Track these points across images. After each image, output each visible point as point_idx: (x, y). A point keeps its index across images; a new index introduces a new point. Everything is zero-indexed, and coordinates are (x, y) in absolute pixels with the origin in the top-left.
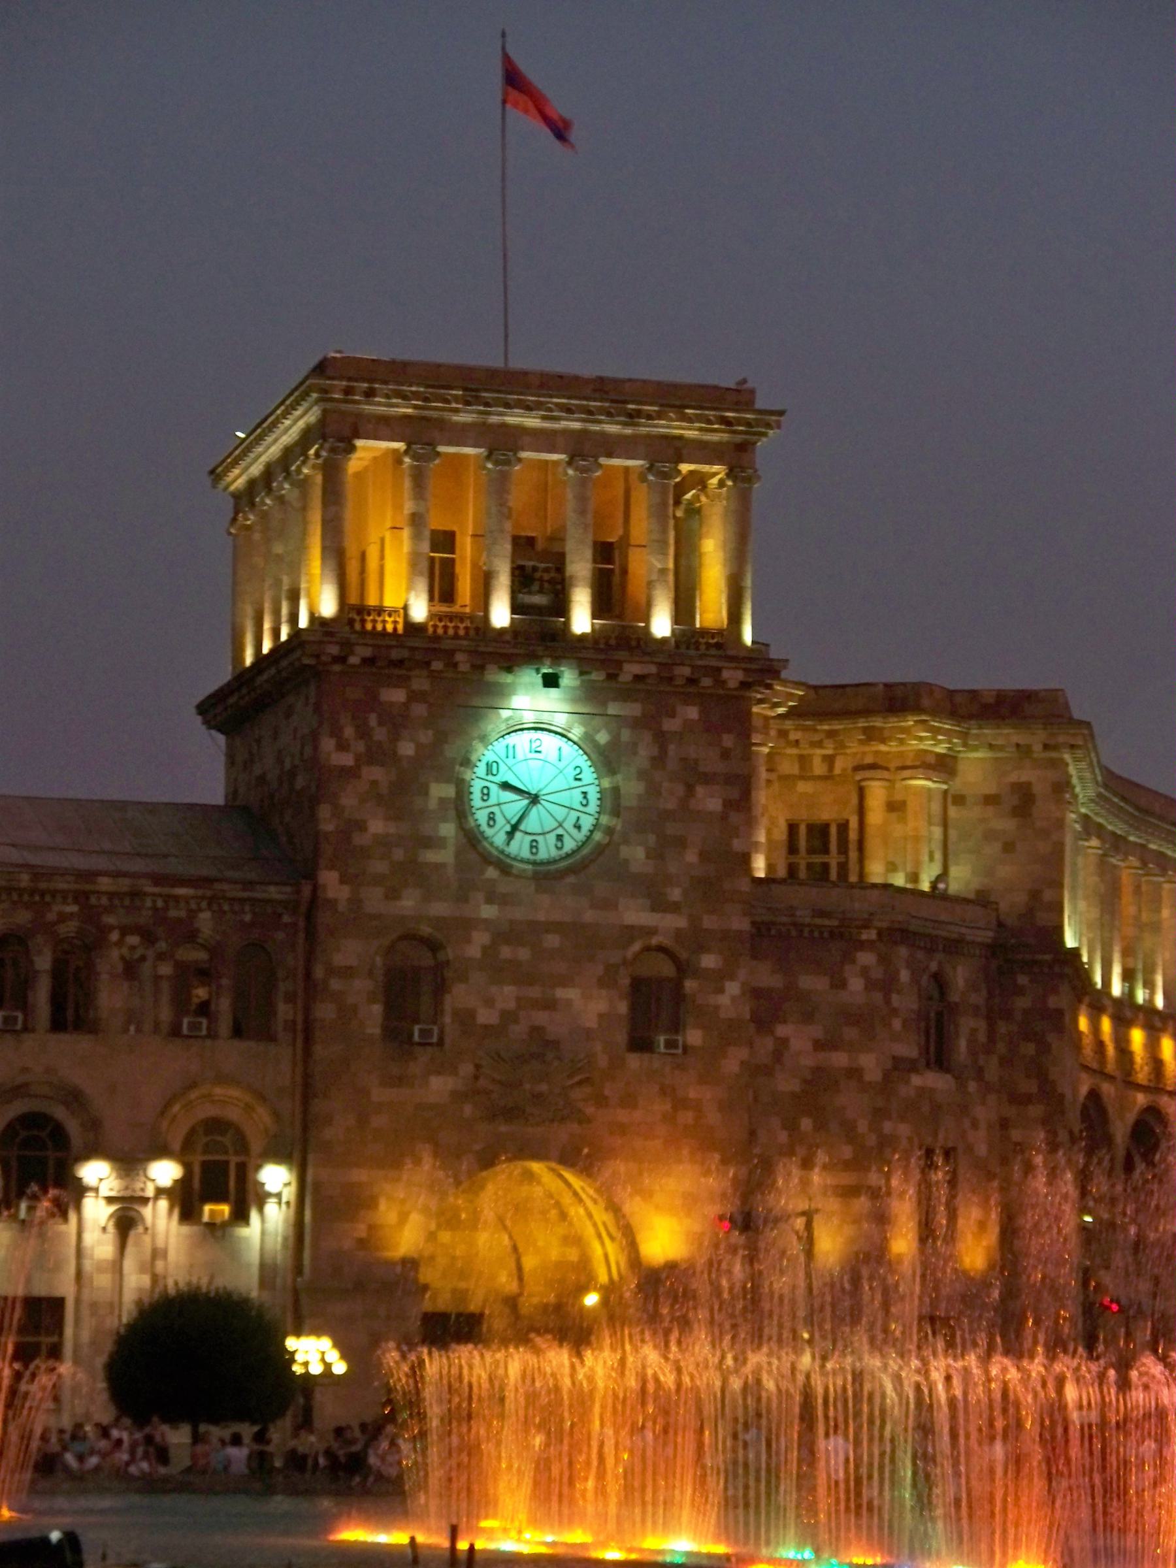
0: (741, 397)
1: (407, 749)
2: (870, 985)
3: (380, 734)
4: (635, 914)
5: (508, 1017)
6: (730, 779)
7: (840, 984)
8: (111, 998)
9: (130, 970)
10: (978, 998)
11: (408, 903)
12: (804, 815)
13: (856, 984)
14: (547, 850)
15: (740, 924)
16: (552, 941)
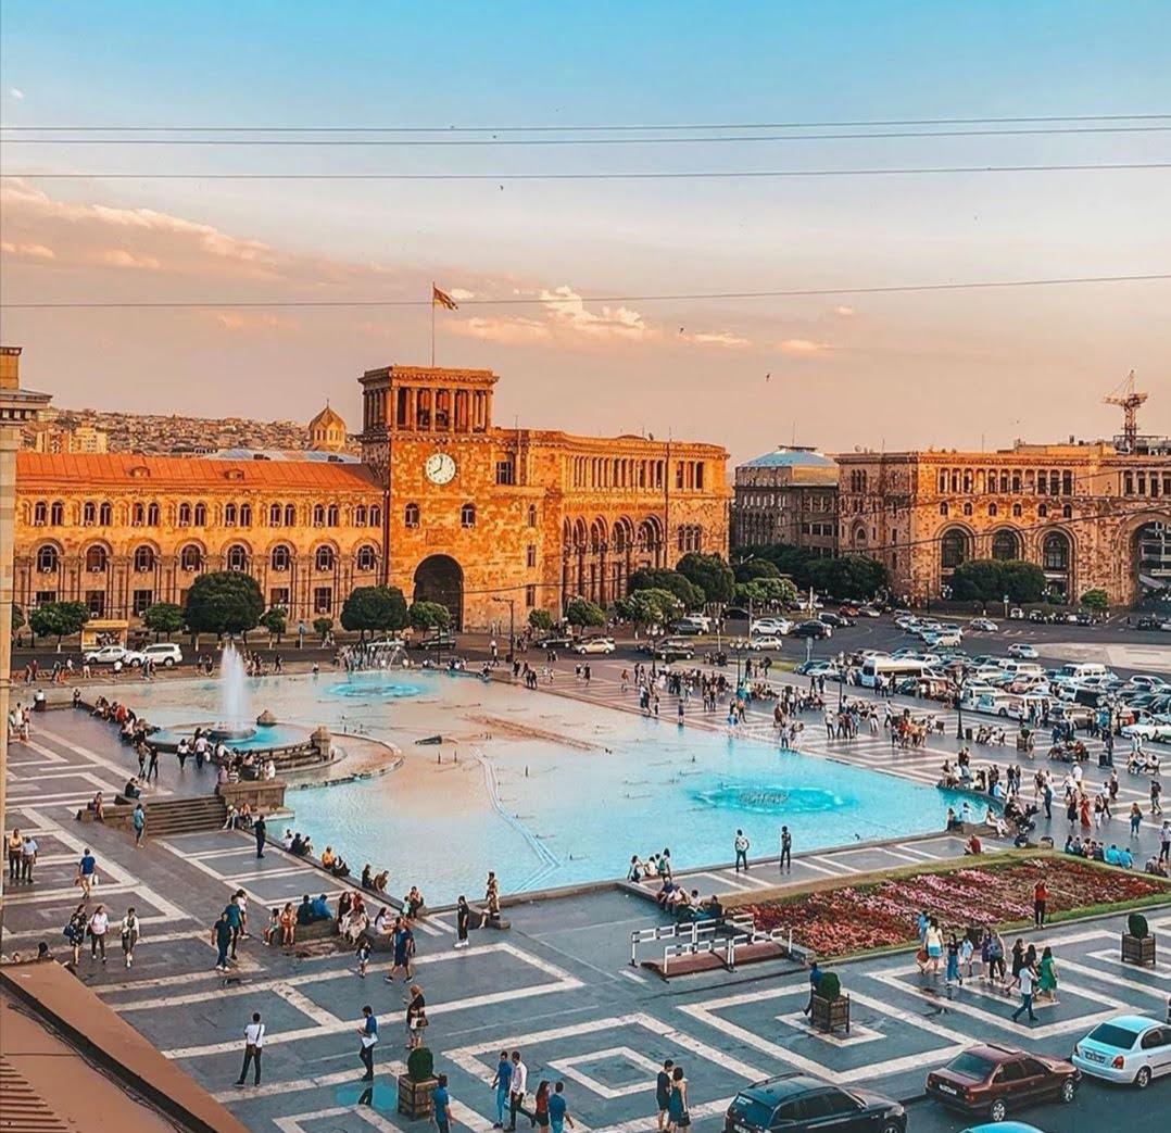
0: (490, 374)
1: (411, 459)
2: (517, 510)
3: (405, 456)
4: (464, 496)
5: (434, 521)
6: (486, 464)
7: (510, 510)
8: (343, 518)
9: (347, 511)
10: (541, 510)
11: (411, 495)
12: (501, 461)
13: (513, 508)
14: (443, 482)
15: (487, 497)
16: (444, 503)
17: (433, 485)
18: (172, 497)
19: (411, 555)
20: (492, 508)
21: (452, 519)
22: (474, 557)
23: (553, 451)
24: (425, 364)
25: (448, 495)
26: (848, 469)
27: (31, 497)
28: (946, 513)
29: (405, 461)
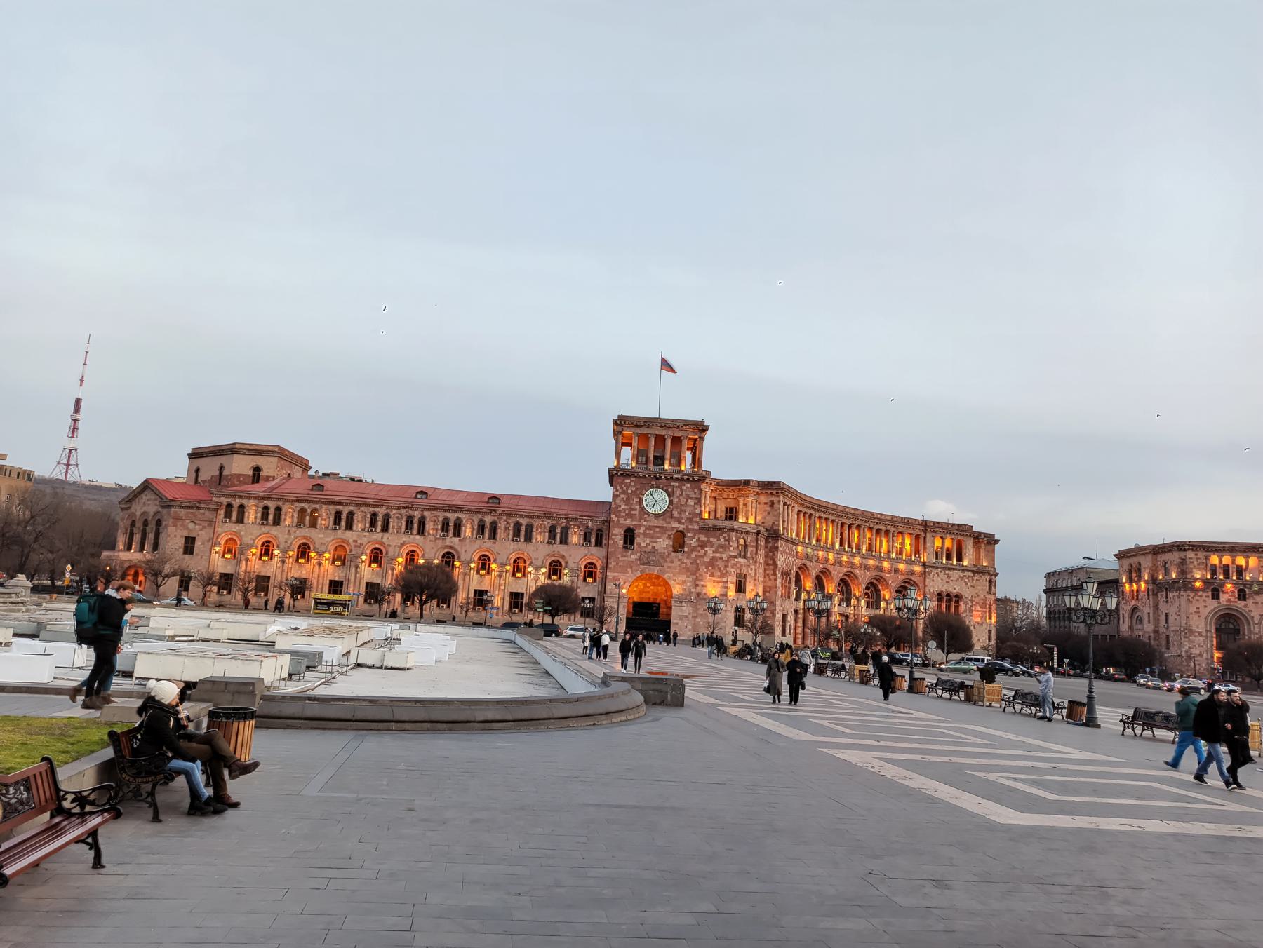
0: (702, 423)
11: (629, 521)
15: (696, 527)
17: (649, 514)
18: (436, 513)
19: (626, 572)
20: (703, 538)
21: (664, 544)
22: (683, 577)
23: (773, 498)
24: (652, 413)
25: (660, 523)
26: (1126, 562)
27: (331, 507)
28: (1218, 598)
29: (625, 493)
